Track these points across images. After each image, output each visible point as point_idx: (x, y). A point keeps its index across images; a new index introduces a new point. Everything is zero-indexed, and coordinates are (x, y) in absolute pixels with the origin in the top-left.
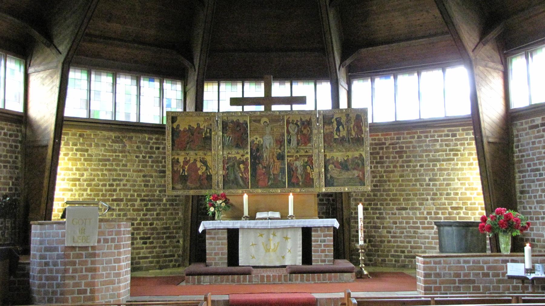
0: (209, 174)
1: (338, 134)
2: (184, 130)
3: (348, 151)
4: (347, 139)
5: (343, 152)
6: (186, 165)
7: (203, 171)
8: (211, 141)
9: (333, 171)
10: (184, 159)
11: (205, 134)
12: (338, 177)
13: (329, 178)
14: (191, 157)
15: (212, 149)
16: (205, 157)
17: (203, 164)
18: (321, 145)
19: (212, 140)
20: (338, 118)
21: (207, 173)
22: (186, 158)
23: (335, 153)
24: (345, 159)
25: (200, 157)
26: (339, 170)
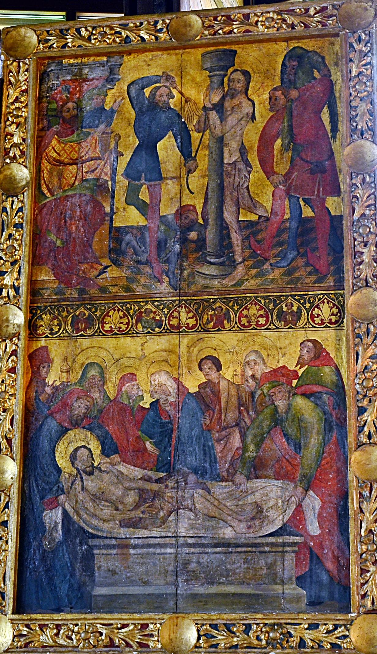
1: (144, 195)
3: (219, 327)
4: (211, 235)
5: (176, 329)
9: (89, 483)
12: (124, 532)
13: (59, 535)
18: (8, 280)
20: (144, 82)
23: (109, 342)
24: (193, 389)
26: (138, 473)
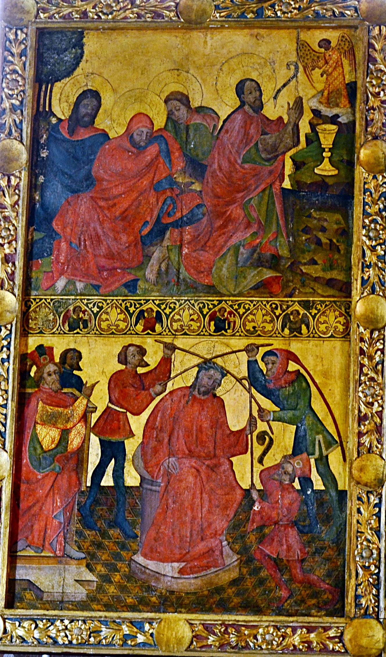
0: (318, 484)
2: (129, 134)
6: (138, 413)
7: (270, 461)
8: (348, 216)
10: (123, 358)
11: (298, 165)
14: (179, 342)
15: (357, 285)
16: (295, 347)
17: (267, 404)
19: (358, 211)
21: (306, 481)
22: (142, 352)
25: (250, 349)
